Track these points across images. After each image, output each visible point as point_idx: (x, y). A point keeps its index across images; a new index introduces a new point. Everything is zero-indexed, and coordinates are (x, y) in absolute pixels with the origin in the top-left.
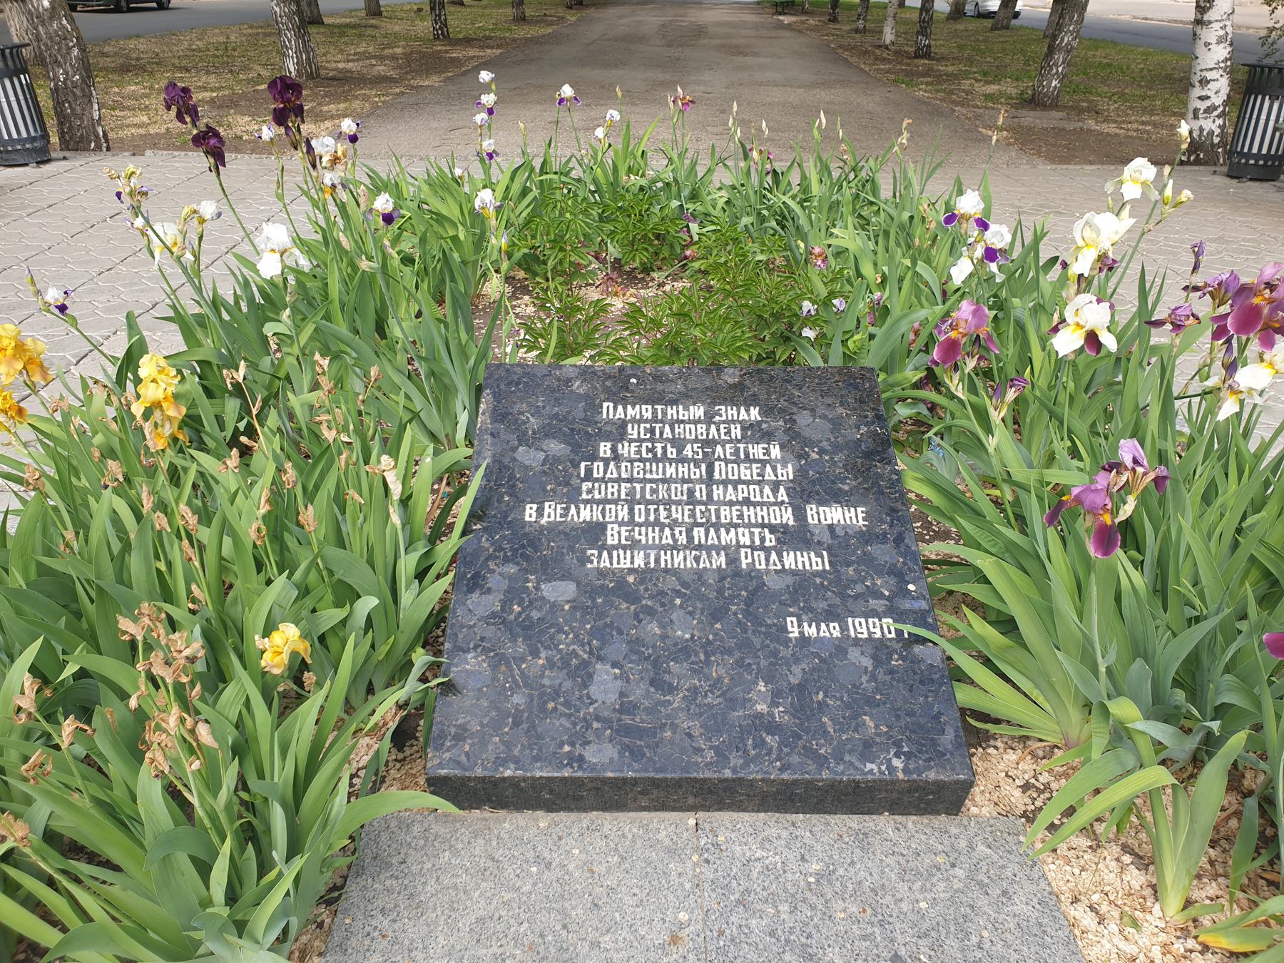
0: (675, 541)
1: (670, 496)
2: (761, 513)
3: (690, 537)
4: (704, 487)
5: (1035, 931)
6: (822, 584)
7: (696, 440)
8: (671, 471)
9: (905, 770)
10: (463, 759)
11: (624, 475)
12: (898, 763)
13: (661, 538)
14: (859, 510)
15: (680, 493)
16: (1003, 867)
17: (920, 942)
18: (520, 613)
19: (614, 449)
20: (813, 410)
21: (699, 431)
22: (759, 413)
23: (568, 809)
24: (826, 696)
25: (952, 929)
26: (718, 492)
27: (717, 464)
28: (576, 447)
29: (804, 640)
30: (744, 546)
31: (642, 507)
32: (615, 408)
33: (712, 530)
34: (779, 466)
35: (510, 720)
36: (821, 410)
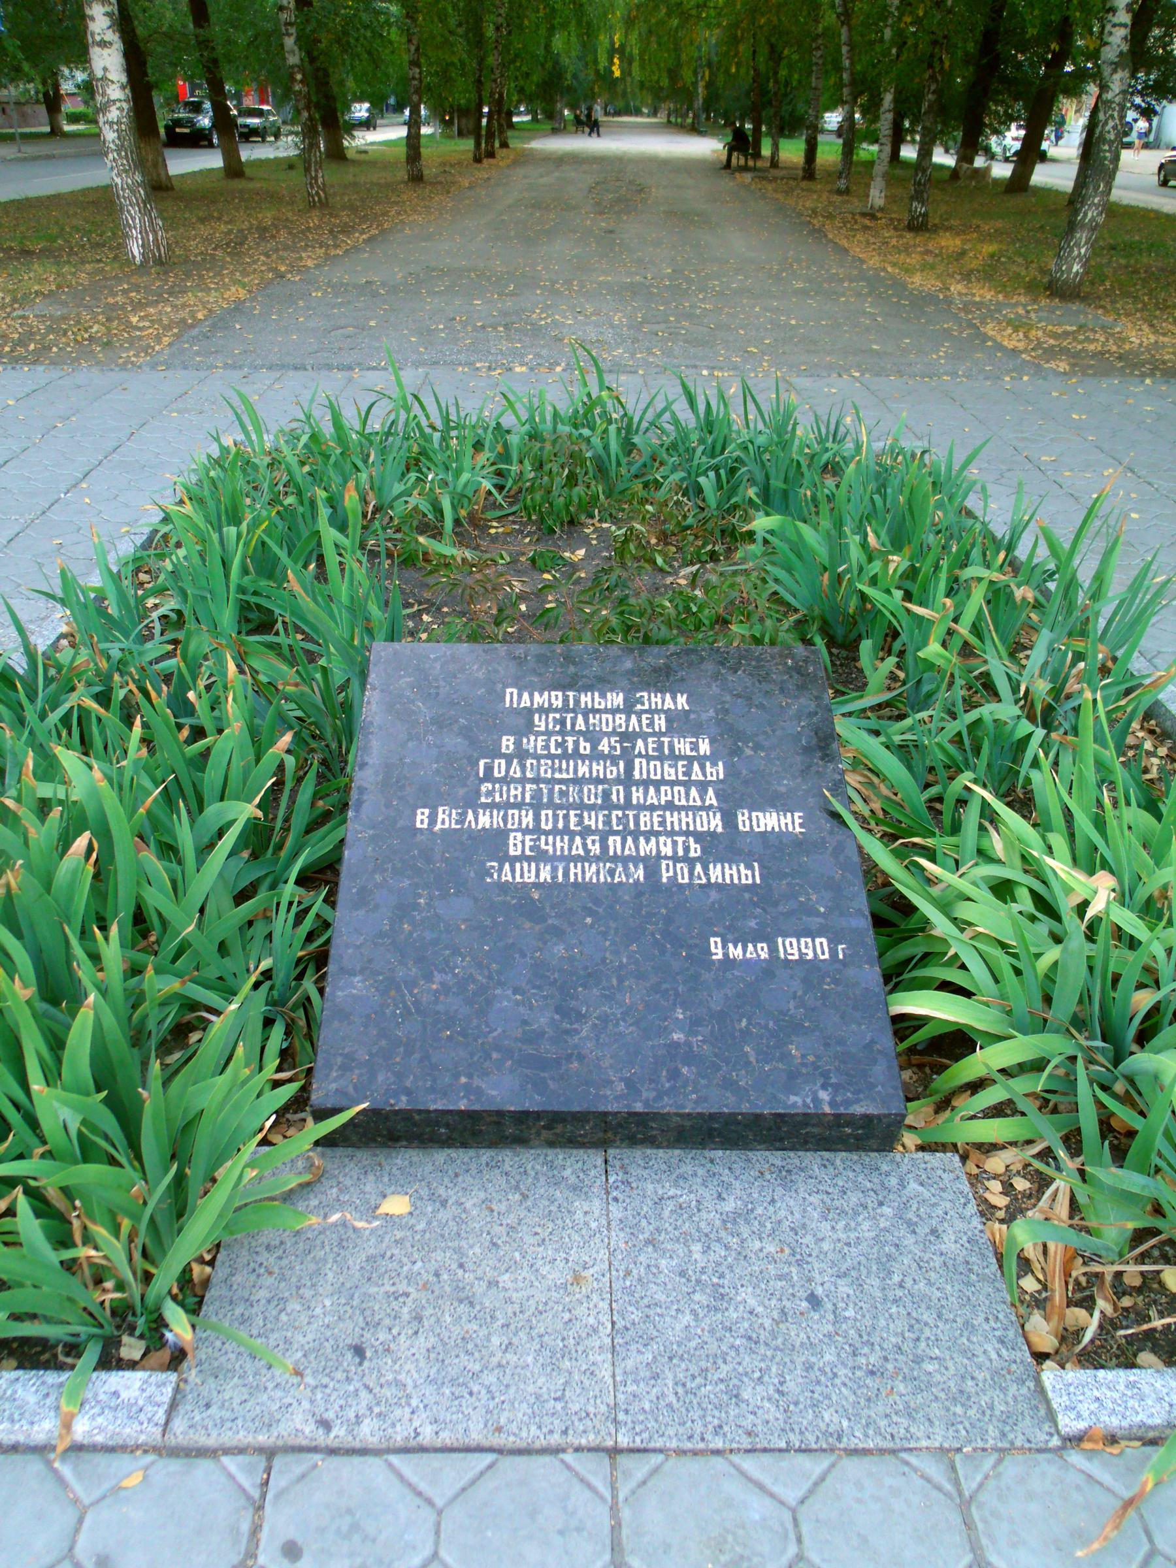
0: (587, 851)
1: (581, 799)
2: (686, 819)
3: (604, 847)
4: (621, 788)
5: (961, 1269)
6: (751, 900)
7: (614, 733)
8: (583, 770)
9: (832, 1104)
10: (351, 1089)
11: (529, 775)
12: (824, 1095)
13: (570, 849)
14: (797, 815)
15: (592, 794)
16: (934, 1205)
17: (839, 1281)
18: (411, 933)
19: (518, 744)
20: (749, 699)
21: (618, 722)
22: (688, 702)
23: (465, 1145)
24: (749, 1023)
25: (874, 1268)
26: (637, 795)
27: (637, 761)
28: (473, 742)
29: (728, 961)
30: (666, 858)
31: (550, 812)
32: (520, 696)
33: (630, 839)
34: (708, 764)
35: (402, 1049)
36: (758, 699)
